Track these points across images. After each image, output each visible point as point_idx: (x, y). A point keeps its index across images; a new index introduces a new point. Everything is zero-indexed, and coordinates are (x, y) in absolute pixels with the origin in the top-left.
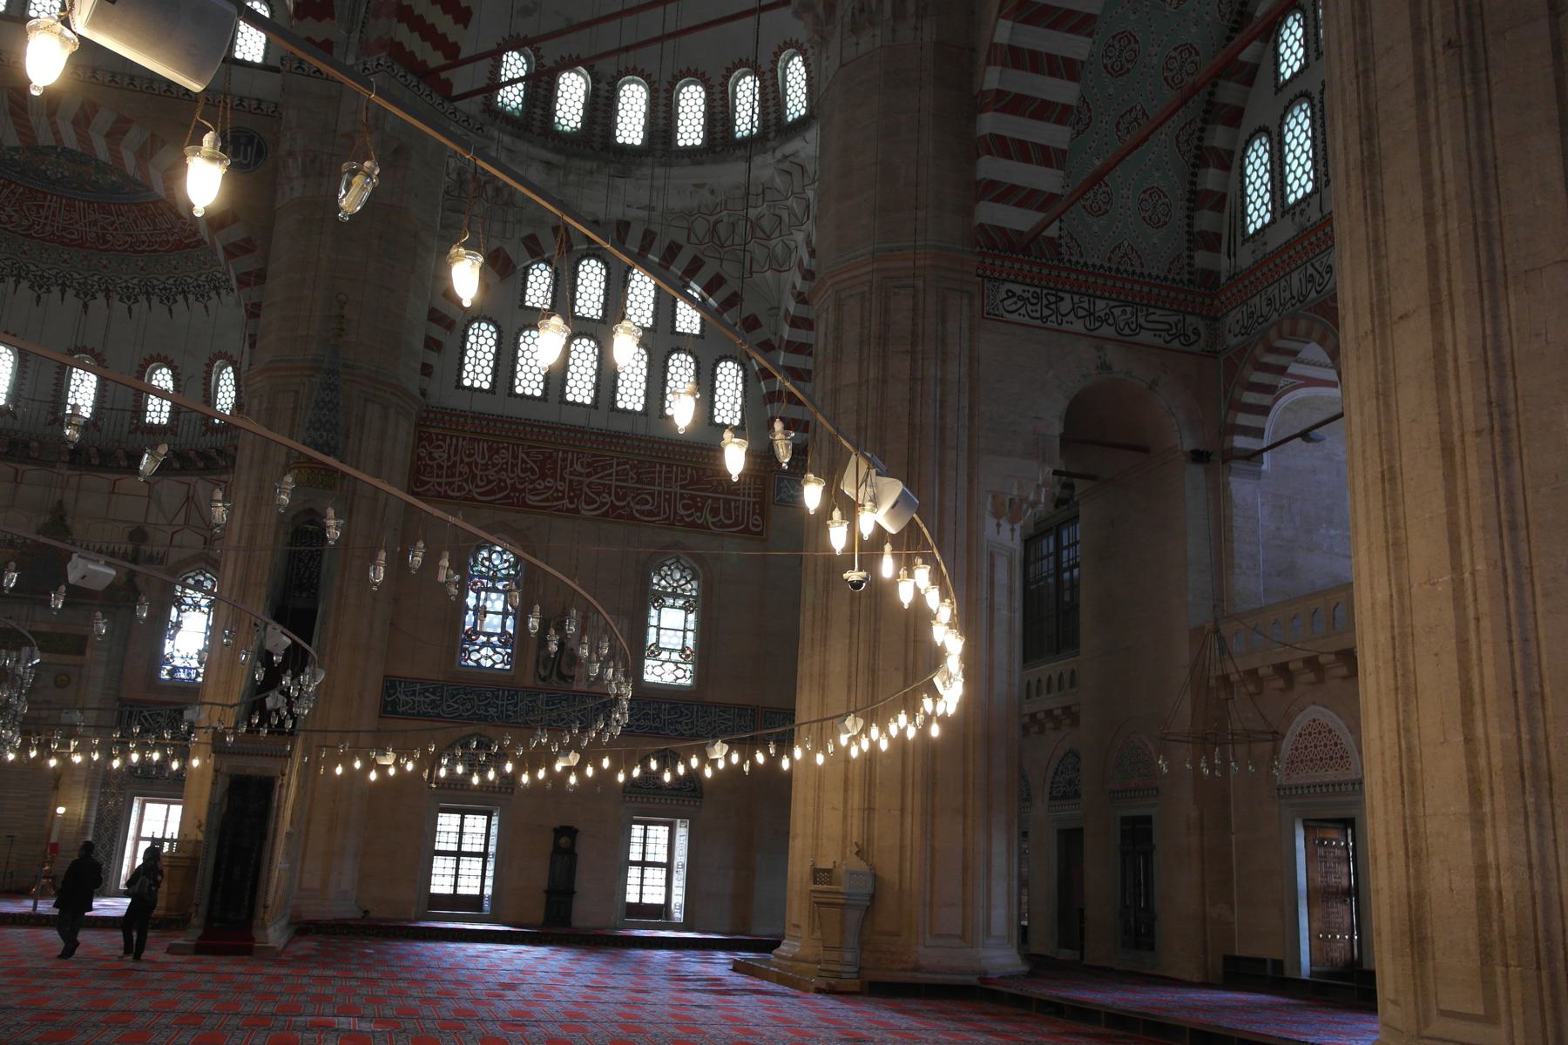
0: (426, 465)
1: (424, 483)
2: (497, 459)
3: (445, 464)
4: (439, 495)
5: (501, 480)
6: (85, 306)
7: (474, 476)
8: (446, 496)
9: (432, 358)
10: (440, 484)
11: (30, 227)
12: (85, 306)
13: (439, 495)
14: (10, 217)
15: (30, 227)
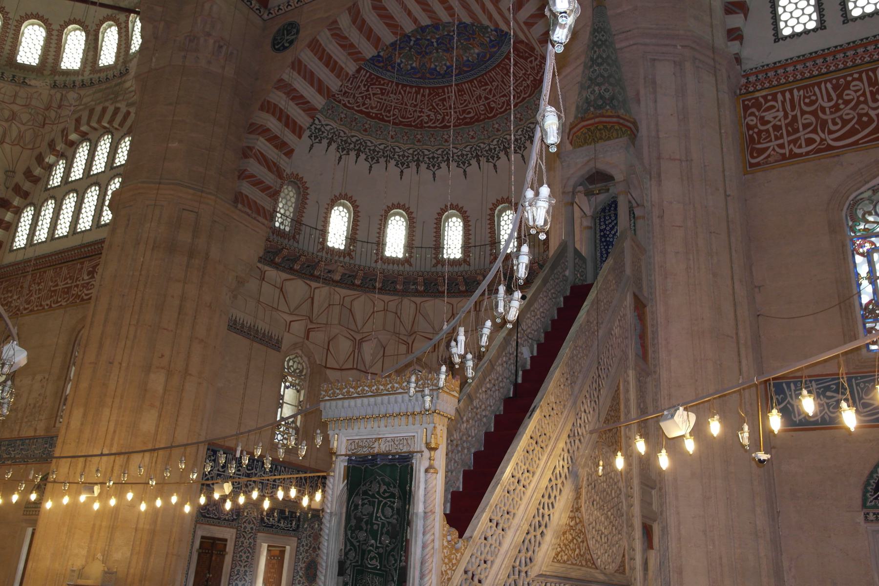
0: (760, 132)
1: (762, 151)
2: (850, 94)
3: (783, 123)
4: (784, 157)
5: (860, 116)
6: (495, 166)
7: (824, 123)
8: (793, 155)
9: (736, 21)
10: (781, 146)
11: (443, 119)
12: (495, 166)
13: (784, 157)
14: (428, 116)
15: (443, 121)
